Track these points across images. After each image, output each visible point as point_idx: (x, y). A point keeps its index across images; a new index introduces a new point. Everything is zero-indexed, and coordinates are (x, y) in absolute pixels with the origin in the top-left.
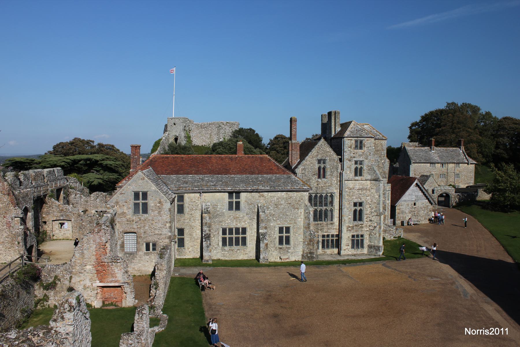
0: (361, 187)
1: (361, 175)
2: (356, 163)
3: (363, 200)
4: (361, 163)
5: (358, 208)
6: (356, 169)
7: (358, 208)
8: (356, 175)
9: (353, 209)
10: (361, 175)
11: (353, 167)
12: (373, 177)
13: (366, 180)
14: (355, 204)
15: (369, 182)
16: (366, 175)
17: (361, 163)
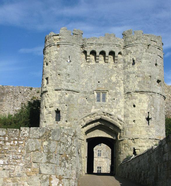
0: (100, 161)
1: (100, 156)
2: (98, 151)
3: (101, 166)
4: (101, 151)
5: (99, 169)
6: (98, 154)
7: (99, 169)
8: (98, 156)
9: (97, 169)
10: (100, 156)
11: (97, 153)
12: (105, 157)
13: (102, 158)
14: (98, 168)
15: (103, 159)
16: (102, 156)
17: (101, 151)
